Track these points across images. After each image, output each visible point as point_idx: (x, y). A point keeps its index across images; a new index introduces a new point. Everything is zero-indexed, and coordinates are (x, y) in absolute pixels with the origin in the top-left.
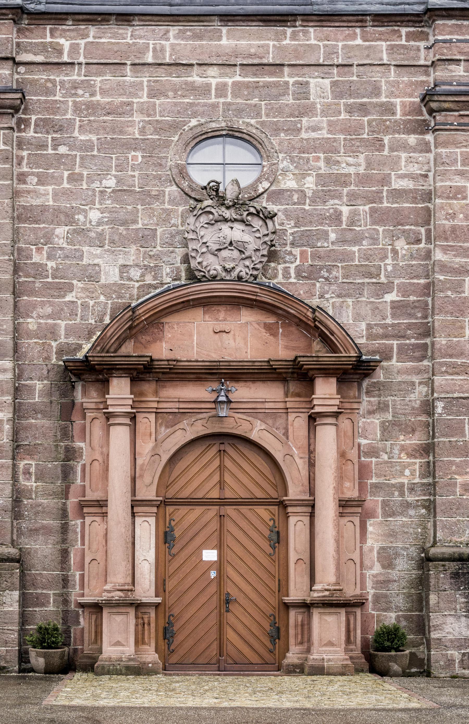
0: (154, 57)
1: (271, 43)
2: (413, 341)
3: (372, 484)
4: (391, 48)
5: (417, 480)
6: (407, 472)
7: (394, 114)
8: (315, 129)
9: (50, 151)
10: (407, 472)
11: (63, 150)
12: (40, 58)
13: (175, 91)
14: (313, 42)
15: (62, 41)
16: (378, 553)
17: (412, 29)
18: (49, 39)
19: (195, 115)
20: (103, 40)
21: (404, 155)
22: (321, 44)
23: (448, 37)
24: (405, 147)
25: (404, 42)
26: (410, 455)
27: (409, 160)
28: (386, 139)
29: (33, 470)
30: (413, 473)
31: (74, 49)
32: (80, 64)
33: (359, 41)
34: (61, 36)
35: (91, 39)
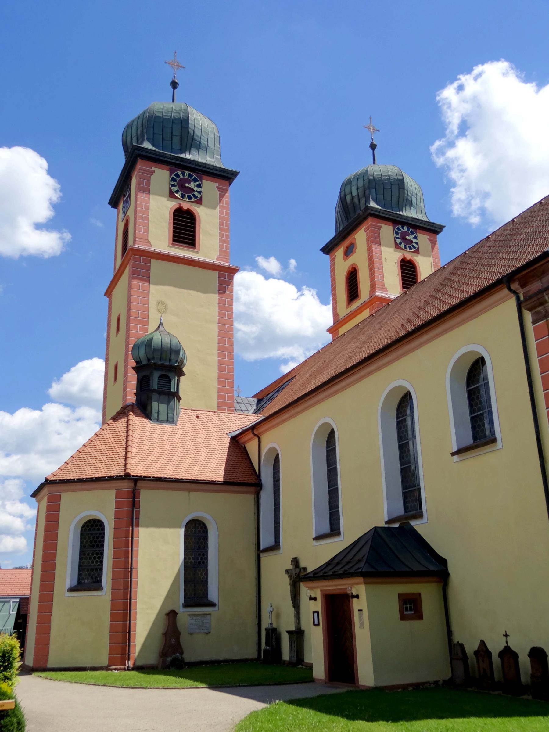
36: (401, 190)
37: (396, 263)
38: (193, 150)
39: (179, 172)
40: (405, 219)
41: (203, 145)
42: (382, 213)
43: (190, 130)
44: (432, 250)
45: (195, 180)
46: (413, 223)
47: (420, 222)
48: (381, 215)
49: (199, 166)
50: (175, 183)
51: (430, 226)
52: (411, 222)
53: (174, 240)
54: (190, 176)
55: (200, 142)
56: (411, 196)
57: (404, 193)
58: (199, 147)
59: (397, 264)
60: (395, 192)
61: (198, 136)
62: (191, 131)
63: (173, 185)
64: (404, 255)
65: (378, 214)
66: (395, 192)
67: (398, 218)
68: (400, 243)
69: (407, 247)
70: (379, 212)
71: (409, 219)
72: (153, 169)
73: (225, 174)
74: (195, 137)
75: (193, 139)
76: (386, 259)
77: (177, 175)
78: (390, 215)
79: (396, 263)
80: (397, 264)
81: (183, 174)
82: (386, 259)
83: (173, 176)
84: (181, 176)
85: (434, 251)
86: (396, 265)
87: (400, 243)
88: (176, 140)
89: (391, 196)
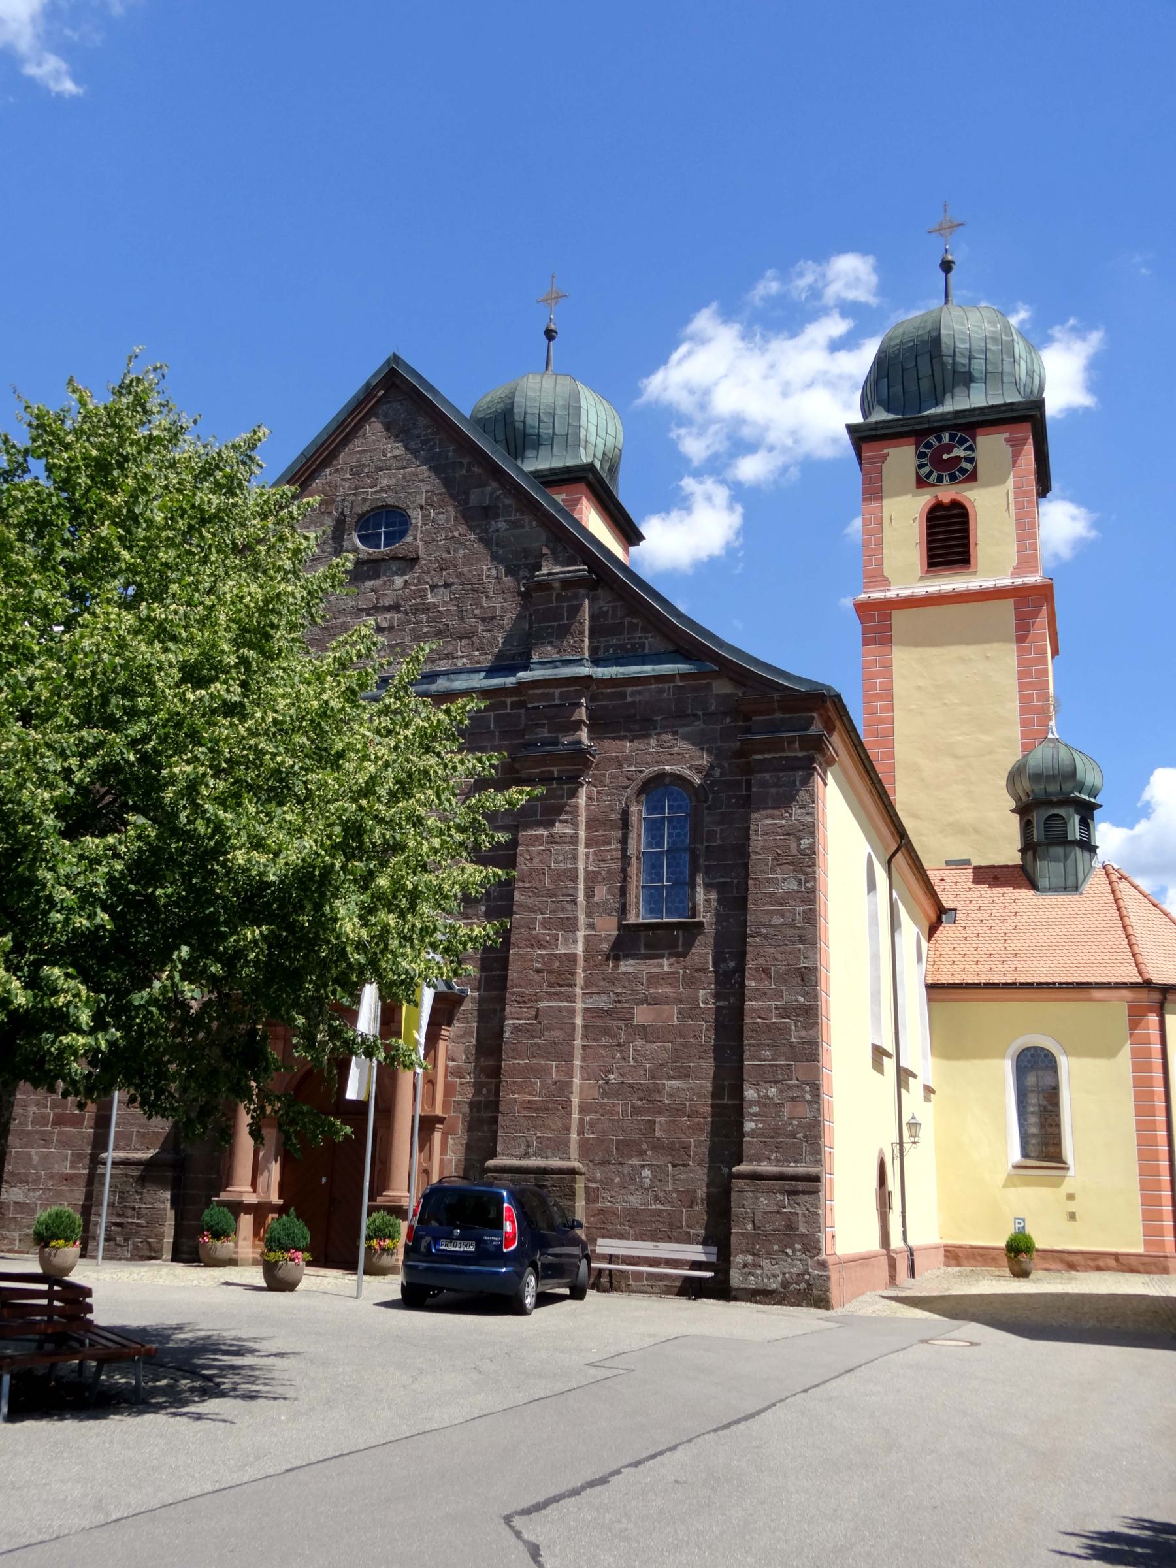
2: (498, 972)
3: (455, 1101)
6: (484, 1091)
10: (484, 1091)
16: (456, 1165)
17: (514, 699)
23: (536, 704)
25: (508, 711)
36: (935, 361)
37: (914, 520)
40: (939, 421)
41: (545, 436)
42: (882, 428)
44: (1014, 462)
45: (962, 441)
46: (959, 421)
47: (977, 412)
48: (880, 432)
51: (1005, 411)
52: (954, 422)
53: (931, 565)
55: (538, 435)
57: (943, 364)
59: (917, 521)
60: (925, 369)
61: (533, 427)
62: (519, 425)
64: (936, 497)
65: (874, 433)
66: (925, 369)
67: (921, 423)
68: (930, 473)
69: (946, 477)
70: (876, 429)
71: (949, 417)
73: (572, 475)
74: (529, 431)
75: (525, 435)
76: (891, 519)
78: (902, 426)
79: (914, 520)
80: (917, 521)
82: (891, 519)
85: (1019, 461)
86: (916, 524)
87: (929, 475)
89: (918, 379)
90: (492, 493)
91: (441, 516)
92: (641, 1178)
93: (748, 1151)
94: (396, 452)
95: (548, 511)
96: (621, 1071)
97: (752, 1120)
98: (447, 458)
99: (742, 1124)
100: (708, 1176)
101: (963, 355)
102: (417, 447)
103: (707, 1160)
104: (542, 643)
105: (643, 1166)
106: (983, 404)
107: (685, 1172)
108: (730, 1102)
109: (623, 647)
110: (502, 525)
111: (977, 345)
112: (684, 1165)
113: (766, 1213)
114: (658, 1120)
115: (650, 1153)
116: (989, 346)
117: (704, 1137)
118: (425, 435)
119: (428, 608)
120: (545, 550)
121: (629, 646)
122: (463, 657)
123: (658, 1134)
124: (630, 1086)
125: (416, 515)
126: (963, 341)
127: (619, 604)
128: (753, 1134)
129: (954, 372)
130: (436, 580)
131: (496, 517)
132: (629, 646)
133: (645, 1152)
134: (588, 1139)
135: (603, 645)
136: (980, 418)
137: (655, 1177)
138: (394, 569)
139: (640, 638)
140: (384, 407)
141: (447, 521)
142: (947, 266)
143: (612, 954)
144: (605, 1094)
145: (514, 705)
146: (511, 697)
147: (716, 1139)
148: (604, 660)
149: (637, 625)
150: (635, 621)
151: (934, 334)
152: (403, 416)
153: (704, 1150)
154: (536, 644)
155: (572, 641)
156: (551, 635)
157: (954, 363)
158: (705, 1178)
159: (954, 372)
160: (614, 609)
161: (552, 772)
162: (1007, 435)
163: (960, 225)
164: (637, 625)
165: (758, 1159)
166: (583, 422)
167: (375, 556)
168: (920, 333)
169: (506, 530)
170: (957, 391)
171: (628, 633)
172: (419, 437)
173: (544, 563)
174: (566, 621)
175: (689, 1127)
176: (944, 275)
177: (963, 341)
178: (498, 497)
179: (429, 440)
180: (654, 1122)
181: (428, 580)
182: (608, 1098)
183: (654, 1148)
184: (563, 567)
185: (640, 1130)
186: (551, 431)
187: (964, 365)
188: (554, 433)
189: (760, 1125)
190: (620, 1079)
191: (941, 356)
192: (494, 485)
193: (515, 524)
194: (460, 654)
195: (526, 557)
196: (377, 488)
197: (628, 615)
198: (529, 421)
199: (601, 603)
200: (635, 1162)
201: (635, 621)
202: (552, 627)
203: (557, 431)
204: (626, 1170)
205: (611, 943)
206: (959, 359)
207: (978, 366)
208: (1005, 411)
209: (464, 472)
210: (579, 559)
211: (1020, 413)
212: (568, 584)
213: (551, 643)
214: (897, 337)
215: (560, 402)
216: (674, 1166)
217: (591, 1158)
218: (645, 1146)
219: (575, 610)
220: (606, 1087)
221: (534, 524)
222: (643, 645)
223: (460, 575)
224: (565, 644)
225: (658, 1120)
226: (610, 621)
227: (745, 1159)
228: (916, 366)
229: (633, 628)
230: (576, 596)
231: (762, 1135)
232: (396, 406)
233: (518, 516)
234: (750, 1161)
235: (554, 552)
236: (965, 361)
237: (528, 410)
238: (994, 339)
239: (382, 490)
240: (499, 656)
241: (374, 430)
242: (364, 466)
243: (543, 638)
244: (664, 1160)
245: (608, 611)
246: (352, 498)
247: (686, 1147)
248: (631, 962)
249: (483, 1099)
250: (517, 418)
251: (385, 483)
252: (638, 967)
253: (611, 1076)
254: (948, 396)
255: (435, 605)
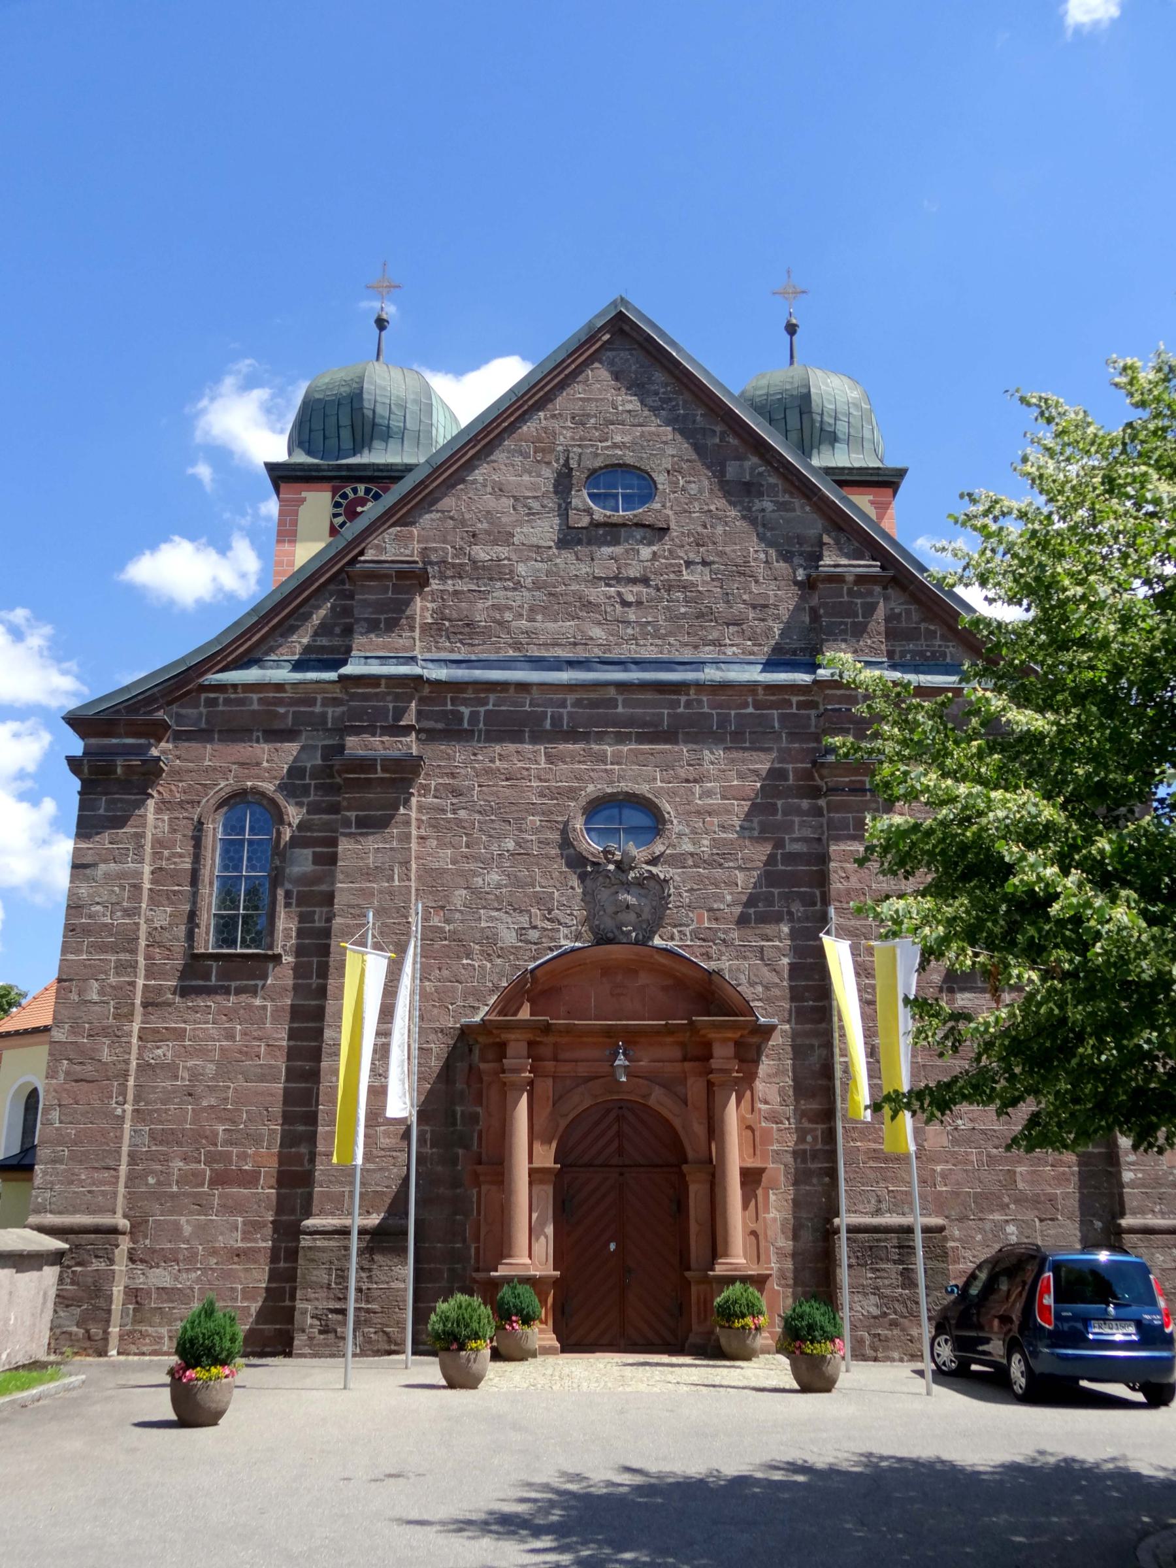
0: (552, 724)
1: (666, 711)
2: (811, 1003)
3: (773, 1151)
4: (783, 718)
5: (819, 1146)
6: (809, 1138)
7: (787, 779)
8: (708, 794)
9: (450, 816)
10: (809, 1138)
11: (462, 814)
12: (440, 726)
13: (573, 758)
14: (706, 710)
15: (462, 709)
18: (450, 707)
19: (592, 781)
20: (503, 708)
21: (797, 819)
22: (714, 712)
23: (837, 706)
24: (799, 812)
26: (811, 1121)
27: (802, 824)
28: (780, 803)
29: (428, 1136)
30: (815, 1138)
31: (474, 716)
32: (480, 731)
33: (750, 710)
34: (462, 705)
35: (490, 707)
36: (804, 416)
38: (377, 444)
39: (348, 490)
41: (395, 429)
43: (365, 411)
49: (381, 471)
50: (340, 510)
51: (872, 475)
54: (368, 491)
55: (388, 427)
56: (832, 421)
57: (812, 421)
58: (387, 434)
61: (383, 417)
62: (368, 413)
63: (335, 515)
72: (304, 494)
74: (378, 420)
75: (374, 425)
77: (344, 496)
81: (355, 491)
83: (337, 498)
84: (351, 495)
88: (346, 434)
90: (752, 469)
91: (693, 485)
92: (1007, 1234)
93: (1130, 1202)
94: (629, 407)
95: (828, 498)
96: (970, 1116)
97: (1131, 1170)
98: (694, 422)
99: (1119, 1174)
100: (1081, 1231)
101: (830, 416)
102: (655, 404)
103: (1078, 1213)
104: (834, 640)
105: (1007, 1221)
106: (848, 465)
107: (1055, 1228)
108: (1096, 1151)
109: (921, 654)
110: (768, 505)
111: (842, 408)
112: (1052, 1220)
113: (1164, 1270)
114: (1019, 1170)
115: (1012, 1206)
116: (852, 410)
117: (1072, 1188)
118: (664, 393)
119: (685, 587)
120: (826, 539)
121: (928, 654)
122: (732, 645)
123: (1021, 1185)
124: (983, 1132)
125: (661, 479)
126: (830, 402)
127: (913, 607)
128: (1133, 1184)
129: (822, 430)
130: (692, 556)
131: (760, 494)
132: (928, 654)
133: (1007, 1205)
134: (941, 1192)
135: (898, 649)
136: (849, 478)
137: (1021, 1233)
138: (638, 537)
139: (940, 646)
140: (609, 354)
141: (701, 491)
142: (791, 329)
143: (945, 986)
144: (955, 1142)
145: (801, 705)
146: (797, 695)
147: (1085, 1191)
148: (903, 666)
149: (935, 632)
150: (932, 627)
151: (804, 391)
152: (634, 367)
153: (1073, 1203)
154: (828, 640)
155: (869, 642)
156: (845, 632)
157: (822, 422)
158: (1078, 1234)
159: (822, 430)
160: (908, 612)
161: (863, 782)
162: (871, 497)
163: (804, 292)
164: (935, 632)
165: (1142, 1212)
166: (434, 421)
167: (614, 520)
168: (788, 387)
169: (774, 511)
170: (823, 448)
171: (926, 640)
172: (657, 393)
173: (826, 553)
174: (861, 619)
175: (1054, 1178)
176: (788, 337)
177: (830, 402)
178: (760, 474)
179: (670, 400)
180: (1015, 1172)
181: (682, 554)
182: (959, 1146)
183: (1017, 1201)
184: (849, 559)
185: (1000, 1181)
186: (402, 425)
187: (830, 424)
188: (405, 428)
189: (1140, 1175)
190: (971, 1125)
191: (810, 412)
192: (755, 459)
193: (783, 506)
194: (728, 641)
195: (801, 544)
196: (609, 443)
197: (923, 620)
198: (379, 410)
199: (893, 605)
200: (997, 1217)
201: (932, 627)
202: (846, 624)
203: (408, 425)
204: (988, 1226)
205: (943, 974)
206: (826, 419)
207: (842, 428)
208: (872, 475)
209: (717, 440)
210: (867, 554)
211: (886, 478)
212: (861, 579)
213: (845, 640)
214: (761, 388)
215: (411, 397)
216: (1041, 1220)
217: (947, 1213)
218: (1006, 1200)
219: (870, 609)
220: (956, 1133)
221: (808, 509)
222: (944, 655)
223: (722, 554)
224: (861, 643)
225: (1019, 1170)
226: (904, 624)
227: (1127, 1211)
228: (785, 418)
229: (931, 635)
230: (870, 593)
231: (1144, 1186)
232: (625, 355)
233: (787, 498)
234: (1134, 1214)
235: (837, 542)
236: (832, 421)
237: (378, 398)
238: (855, 405)
239: (615, 446)
240: (777, 649)
241: (599, 377)
242: (588, 415)
243: (836, 635)
244: (1030, 1215)
245: (900, 614)
246: (578, 450)
247: (1052, 1199)
248: (967, 995)
249: (808, 1147)
250: (366, 404)
251: (618, 439)
252: (977, 1002)
253: (960, 1122)
254: (815, 451)
255: (693, 584)
